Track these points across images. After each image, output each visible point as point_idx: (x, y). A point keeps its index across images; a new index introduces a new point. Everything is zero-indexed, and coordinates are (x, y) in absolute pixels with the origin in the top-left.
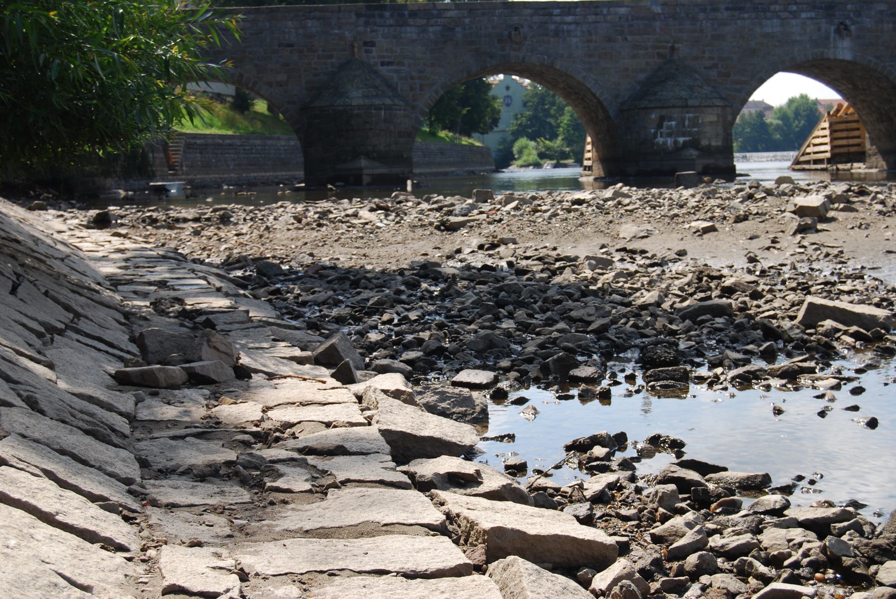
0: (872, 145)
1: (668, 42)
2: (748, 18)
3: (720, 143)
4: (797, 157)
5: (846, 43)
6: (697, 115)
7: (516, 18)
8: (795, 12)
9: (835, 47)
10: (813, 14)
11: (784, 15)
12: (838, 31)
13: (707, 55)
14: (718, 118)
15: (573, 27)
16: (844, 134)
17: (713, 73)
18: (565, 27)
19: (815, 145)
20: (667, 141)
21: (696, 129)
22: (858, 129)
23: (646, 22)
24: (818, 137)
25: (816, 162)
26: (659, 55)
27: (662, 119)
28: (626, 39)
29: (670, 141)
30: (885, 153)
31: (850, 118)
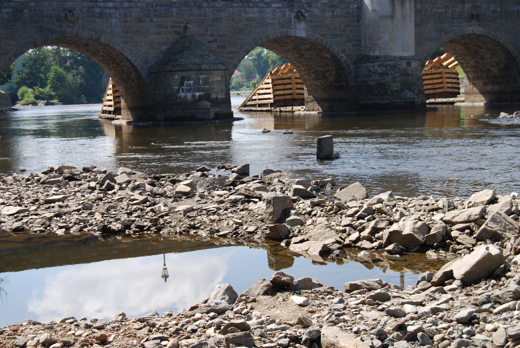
0: (309, 95)
1: (182, 23)
2: (237, 7)
3: (223, 96)
4: (245, 102)
5: (302, 25)
6: (208, 76)
7: (70, 3)
8: (268, 3)
9: (295, 28)
10: (280, 5)
11: (260, 5)
12: (297, 17)
13: (209, 33)
14: (222, 78)
15: (113, 11)
16: (282, 87)
17: (214, 46)
18: (107, 11)
19: (259, 94)
20: (187, 95)
21: (207, 86)
22: (290, 84)
23: (166, 8)
24: (263, 89)
25: (260, 105)
26: (176, 32)
27: (183, 79)
28: (152, 20)
29: (189, 95)
30: (319, 101)
31: (285, 76)
